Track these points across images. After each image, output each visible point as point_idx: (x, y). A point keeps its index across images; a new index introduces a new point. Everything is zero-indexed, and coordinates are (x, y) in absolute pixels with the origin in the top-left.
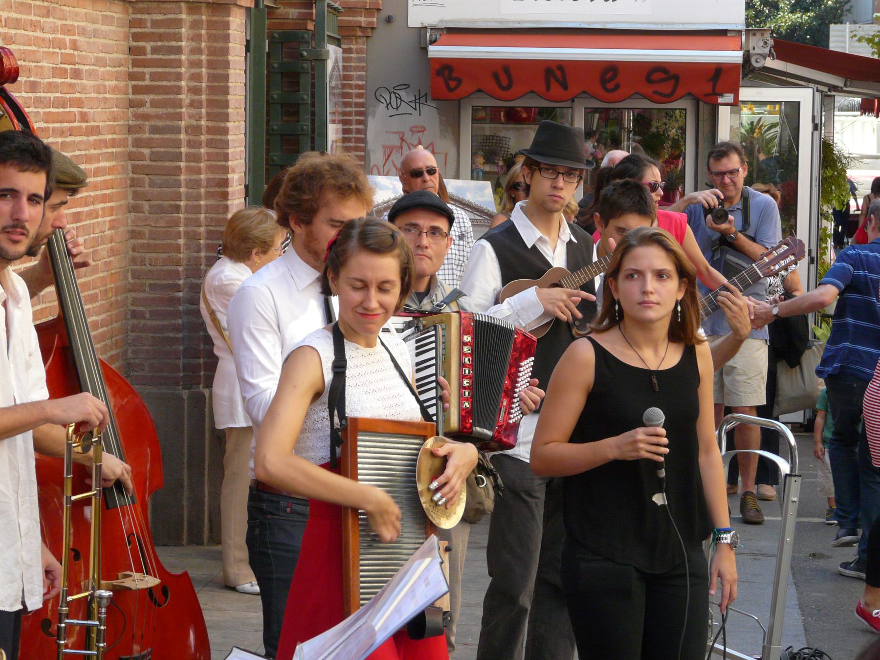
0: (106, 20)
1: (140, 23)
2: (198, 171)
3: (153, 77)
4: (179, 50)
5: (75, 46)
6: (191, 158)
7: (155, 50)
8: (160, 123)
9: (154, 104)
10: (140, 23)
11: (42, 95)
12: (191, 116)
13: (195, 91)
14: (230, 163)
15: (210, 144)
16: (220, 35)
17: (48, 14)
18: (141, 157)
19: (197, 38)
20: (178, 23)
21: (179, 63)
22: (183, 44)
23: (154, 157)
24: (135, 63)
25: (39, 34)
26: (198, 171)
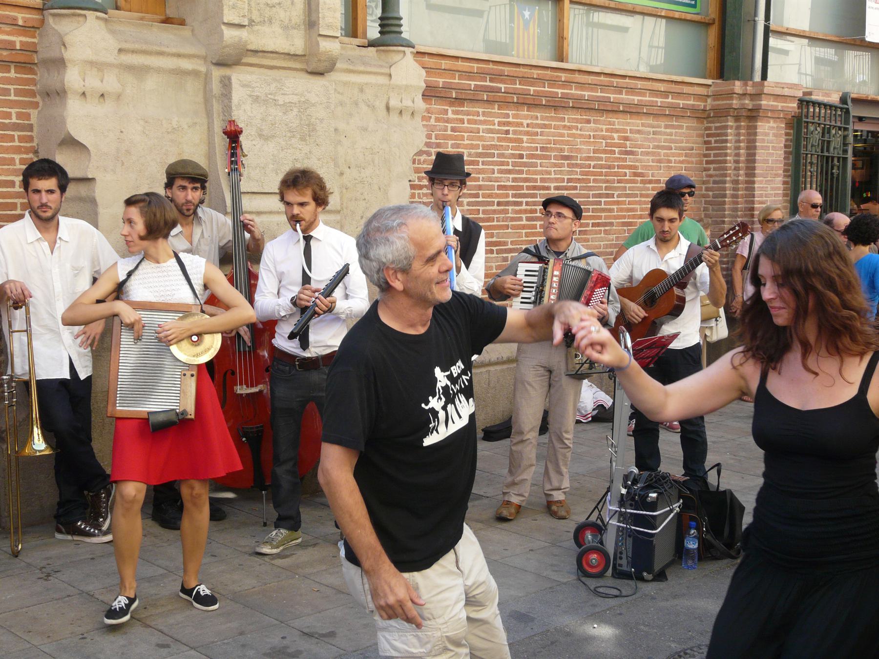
0: (681, 127)
1: (709, 128)
2: (737, 203)
3: (715, 155)
4: (726, 141)
5: (626, 139)
6: (733, 196)
7: (716, 142)
8: (717, 179)
9: (715, 169)
10: (709, 128)
11: (579, 162)
12: (735, 175)
13: (737, 162)
14: (756, 199)
15: (746, 189)
16: (752, 132)
17: (588, 122)
18: (708, 196)
19: (738, 135)
20: (726, 127)
21: (726, 148)
22: (729, 138)
23: (715, 196)
24: (707, 149)
25: (574, 131)
26: (737, 203)
